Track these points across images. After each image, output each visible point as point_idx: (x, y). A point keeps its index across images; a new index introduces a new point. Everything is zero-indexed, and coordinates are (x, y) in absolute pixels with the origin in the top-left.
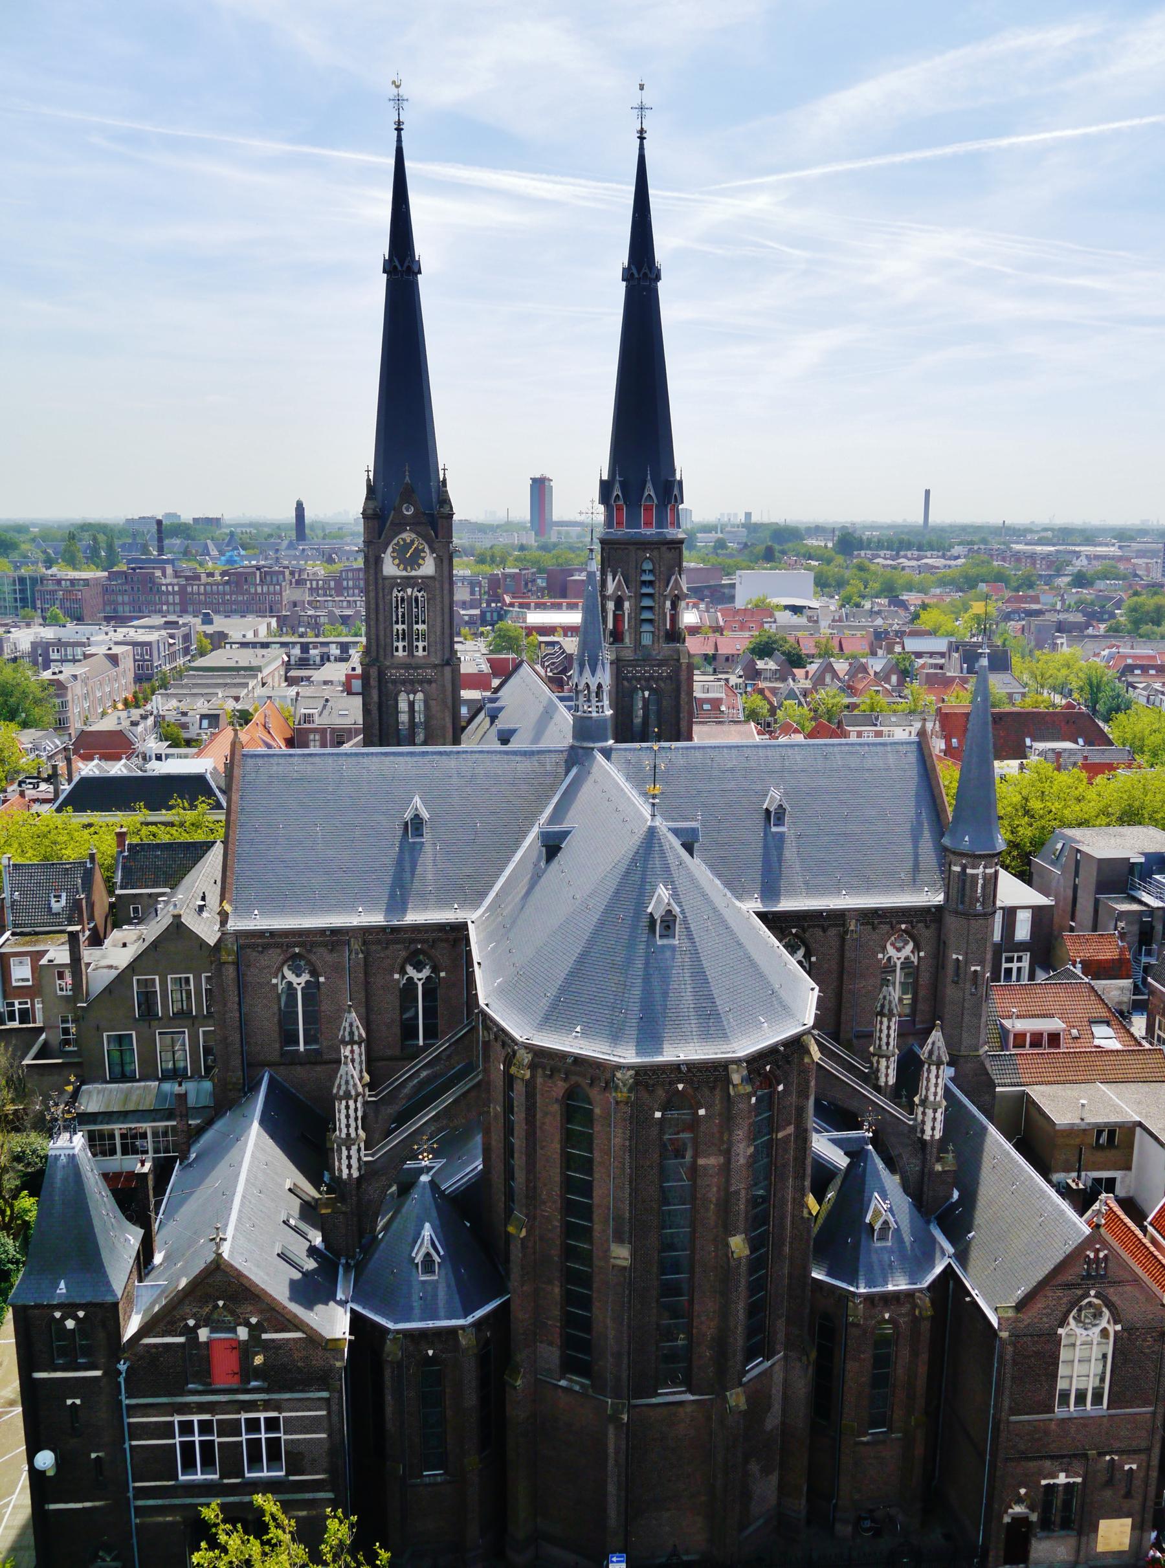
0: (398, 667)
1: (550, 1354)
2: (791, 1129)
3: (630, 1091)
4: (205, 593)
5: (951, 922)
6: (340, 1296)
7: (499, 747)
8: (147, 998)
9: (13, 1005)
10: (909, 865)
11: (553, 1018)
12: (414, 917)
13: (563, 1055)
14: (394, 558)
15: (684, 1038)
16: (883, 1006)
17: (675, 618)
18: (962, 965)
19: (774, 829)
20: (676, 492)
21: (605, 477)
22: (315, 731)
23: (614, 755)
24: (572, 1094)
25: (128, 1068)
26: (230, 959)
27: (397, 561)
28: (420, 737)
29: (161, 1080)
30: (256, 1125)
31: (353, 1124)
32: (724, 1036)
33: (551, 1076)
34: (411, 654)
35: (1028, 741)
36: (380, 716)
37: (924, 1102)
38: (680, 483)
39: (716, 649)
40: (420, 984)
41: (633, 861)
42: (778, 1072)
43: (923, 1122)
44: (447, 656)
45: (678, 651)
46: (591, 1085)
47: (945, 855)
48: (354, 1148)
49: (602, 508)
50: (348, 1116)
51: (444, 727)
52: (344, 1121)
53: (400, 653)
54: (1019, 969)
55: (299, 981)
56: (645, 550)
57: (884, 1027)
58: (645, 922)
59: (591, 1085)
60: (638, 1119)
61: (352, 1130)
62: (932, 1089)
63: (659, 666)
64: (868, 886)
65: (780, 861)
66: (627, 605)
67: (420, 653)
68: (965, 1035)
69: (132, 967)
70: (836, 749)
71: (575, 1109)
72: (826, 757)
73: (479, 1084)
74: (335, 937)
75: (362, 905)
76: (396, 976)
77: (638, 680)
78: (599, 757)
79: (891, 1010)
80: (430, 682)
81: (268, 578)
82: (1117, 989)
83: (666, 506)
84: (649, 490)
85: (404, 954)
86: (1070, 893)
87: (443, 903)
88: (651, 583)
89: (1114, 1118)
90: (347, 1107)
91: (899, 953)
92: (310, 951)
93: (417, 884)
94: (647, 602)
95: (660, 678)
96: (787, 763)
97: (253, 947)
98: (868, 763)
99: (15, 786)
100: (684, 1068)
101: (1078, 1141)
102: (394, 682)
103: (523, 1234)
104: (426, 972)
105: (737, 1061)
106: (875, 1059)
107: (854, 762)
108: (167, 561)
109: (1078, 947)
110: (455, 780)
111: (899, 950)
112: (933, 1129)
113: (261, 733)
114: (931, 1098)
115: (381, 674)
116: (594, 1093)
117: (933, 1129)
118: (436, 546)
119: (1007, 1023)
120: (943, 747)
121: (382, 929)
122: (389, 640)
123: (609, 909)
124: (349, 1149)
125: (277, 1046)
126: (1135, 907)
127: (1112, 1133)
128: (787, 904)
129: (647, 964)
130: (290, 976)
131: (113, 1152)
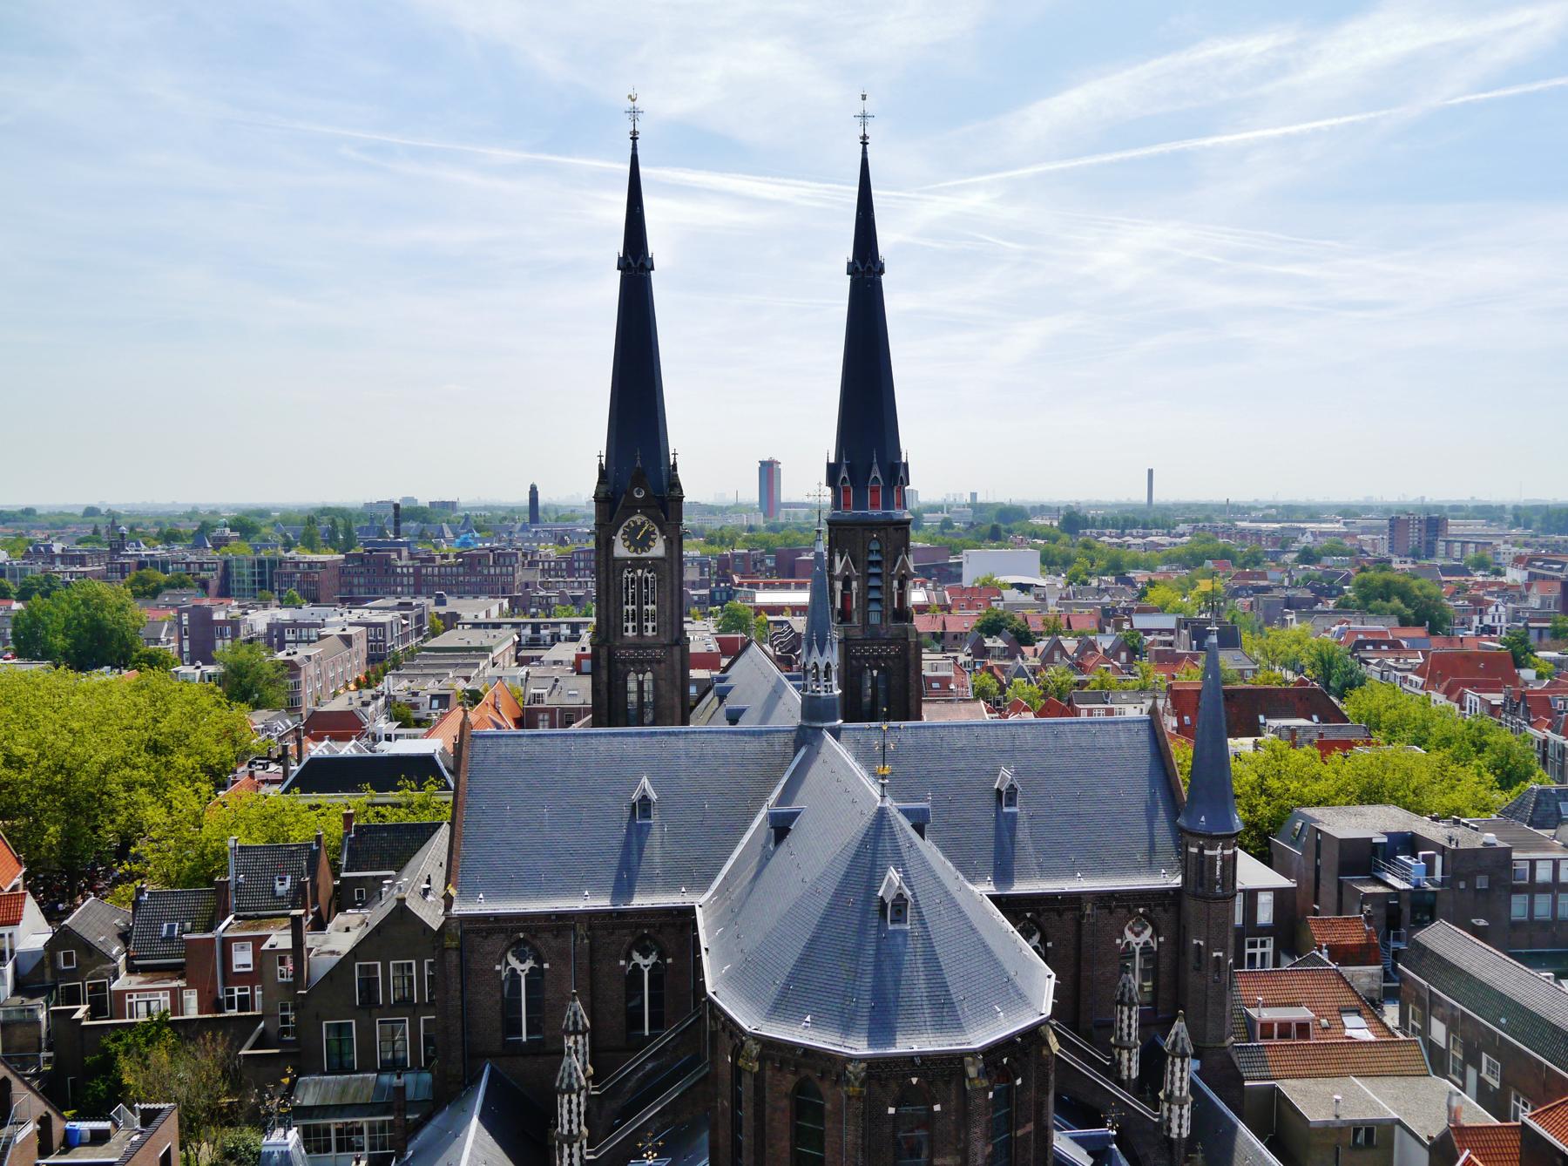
0: (629, 647)
2: (1030, 1127)
3: (862, 1084)
4: (439, 575)
5: (1191, 906)
7: (727, 727)
8: (369, 985)
9: (232, 991)
10: (1145, 846)
11: (782, 1007)
12: (640, 901)
13: (793, 1047)
15: (917, 1029)
16: (1123, 994)
17: (903, 597)
18: (1204, 951)
19: (1006, 810)
20: (902, 474)
21: (832, 460)
22: (544, 710)
23: (843, 735)
24: (802, 1088)
26: (454, 944)
28: (649, 717)
29: (379, 1072)
30: (475, 1120)
31: (575, 1120)
32: (958, 1027)
33: (780, 1069)
35: (1262, 719)
36: (609, 699)
37: (1169, 1097)
38: (906, 465)
40: (646, 971)
41: (863, 843)
42: (1015, 1065)
43: (1169, 1119)
44: (676, 635)
45: (906, 630)
46: (822, 1078)
47: (1182, 836)
48: (576, 1145)
49: (829, 490)
50: (570, 1112)
52: (566, 1116)
53: (630, 633)
54: (1263, 955)
55: (523, 968)
56: (872, 531)
57: (1125, 1017)
58: (875, 906)
59: (822, 1078)
60: (872, 1115)
61: (574, 1127)
62: (1177, 1084)
64: (1103, 869)
65: (1013, 843)
66: (854, 584)
67: (650, 633)
68: (1210, 1025)
69: (355, 953)
70: (1067, 728)
71: (805, 1105)
72: (1056, 736)
73: (706, 1076)
76: (622, 963)
78: (828, 737)
79: (1131, 999)
80: (659, 662)
82: (1365, 975)
84: (876, 473)
85: (629, 939)
86: (1312, 875)
87: (671, 887)
88: (878, 563)
89: (1370, 1116)
90: (570, 1102)
91: (1137, 938)
92: (534, 937)
93: (644, 867)
94: (874, 582)
95: (888, 657)
97: (478, 932)
98: (1100, 742)
99: (245, 767)
100: (918, 1061)
102: (624, 662)
104: (652, 959)
105: (973, 1053)
106: (1116, 1051)
107: (1084, 741)
108: (403, 544)
109: (1324, 931)
110: (683, 761)
111: (1137, 935)
112: (1180, 1126)
113: (490, 713)
114: (1177, 1093)
115: (611, 654)
116: (825, 1087)
117: (1180, 1126)
119: (1253, 1012)
121: (608, 913)
123: (837, 895)
124: (570, 1147)
125: (499, 1035)
126: (1380, 889)
127: (1369, 1132)
128: (1020, 888)
129: (878, 950)
130: (514, 962)
131: (328, 1149)
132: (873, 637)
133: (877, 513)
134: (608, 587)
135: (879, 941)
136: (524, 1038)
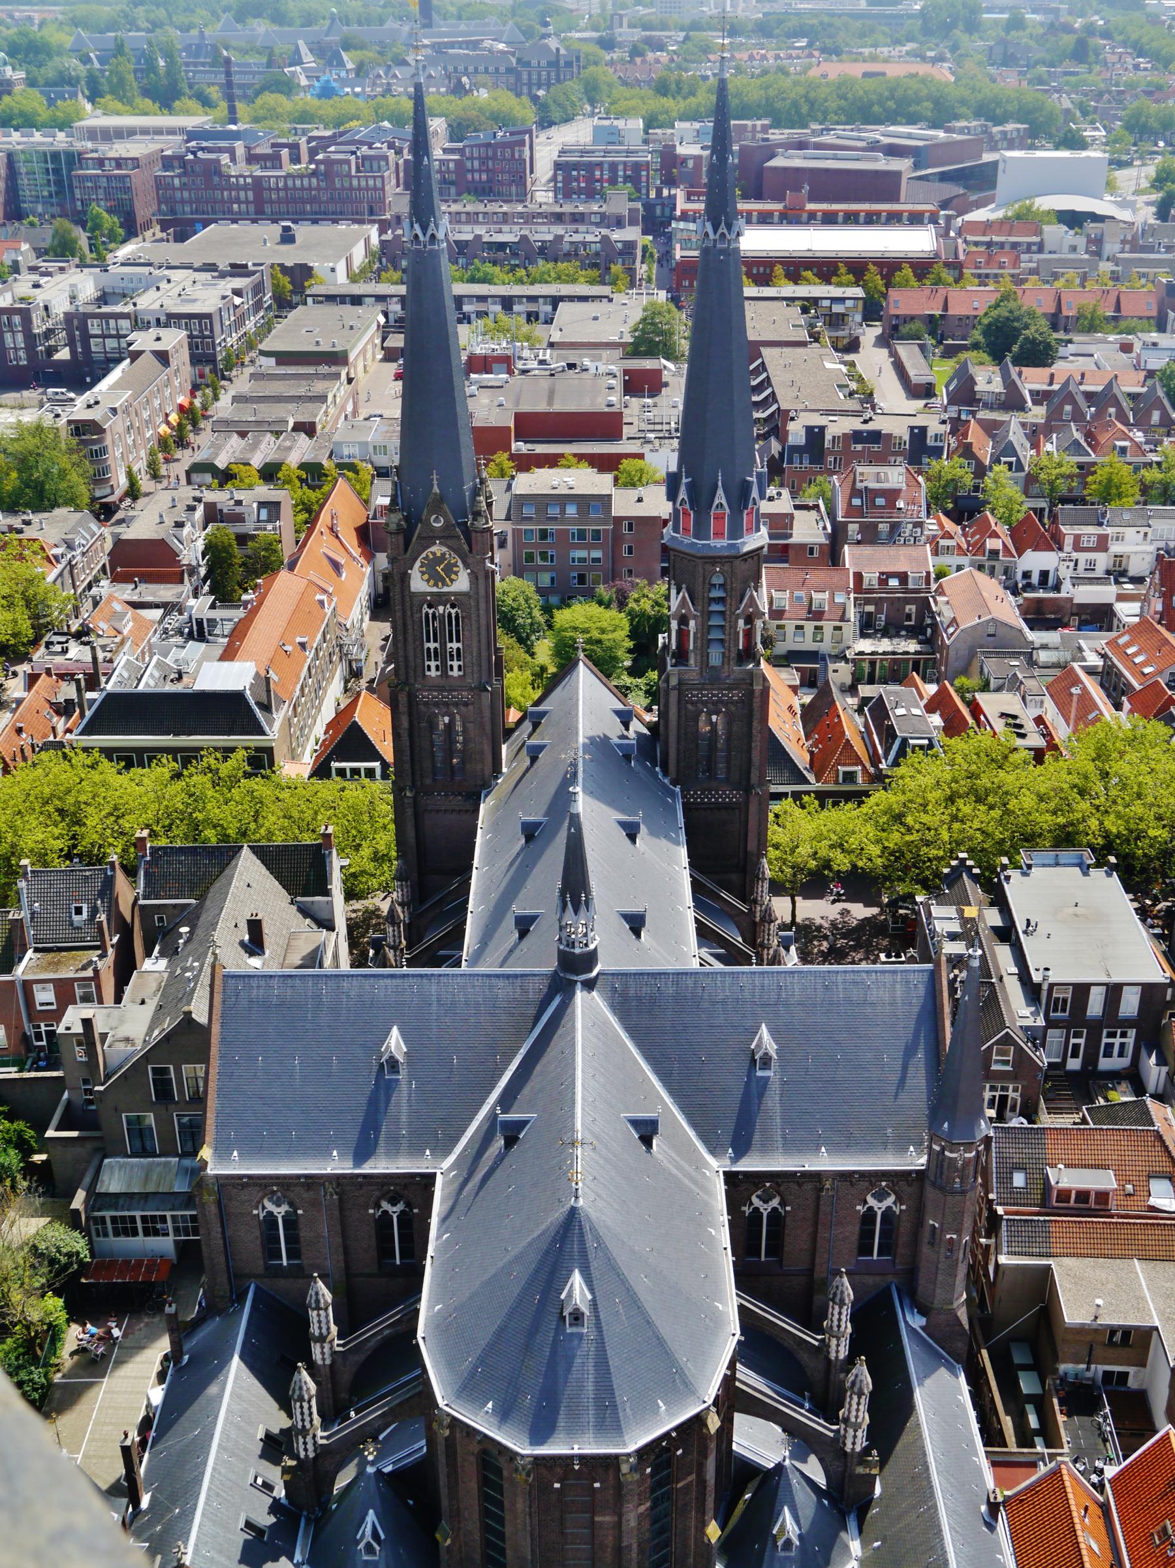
2: (693, 1476)
3: (528, 1475)
4: (286, 188)
6: (298, 1557)
11: (469, 1389)
14: (423, 573)
16: (835, 1294)
21: (673, 468)
25: (148, 1144)
27: (426, 577)
30: (236, 1360)
37: (846, 1420)
39: (945, 308)
41: (554, 1241)
48: (309, 1439)
50: (302, 1414)
51: (482, 753)
53: (433, 673)
54: (1122, 1045)
56: (714, 564)
62: (854, 1413)
63: (730, 689)
66: (692, 623)
67: (456, 673)
68: (938, 1291)
73: (420, 1393)
74: (311, 1181)
75: (336, 1148)
77: (705, 703)
80: (466, 704)
81: (367, 164)
83: (741, 512)
84: (720, 497)
87: (416, 1150)
88: (720, 600)
89: (1132, 1321)
96: (784, 995)
97: (234, 1186)
98: (873, 996)
101: (1089, 1338)
103: (449, 1541)
104: (400, 1207)
108: (236, 136)
114: (853, 1420)
118: (470, 561)
120: (1159, 608)
122: (419, 661)
125: (261, 1262)
130: (270, 1207)
131: (135, 1234)
132: (712, 677)
133: (719, 544)
134: (405, 624)
135: (555, 1342)
136: (285, 1263)
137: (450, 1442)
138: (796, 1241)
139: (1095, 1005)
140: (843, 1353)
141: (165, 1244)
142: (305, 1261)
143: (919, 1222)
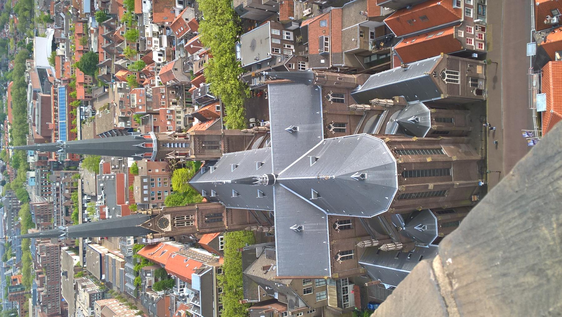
1: (441, 199)
34: (194, 220)
55: (340, 256)
66: (177, 152)
108: (34, 291)
130: (339, 259)
137: (397, 208)
138: (341, 120)
139: (278, 42)
140: (368, 106)
141: (350, 287)
142: (352, 249)
143: (335, 87)
